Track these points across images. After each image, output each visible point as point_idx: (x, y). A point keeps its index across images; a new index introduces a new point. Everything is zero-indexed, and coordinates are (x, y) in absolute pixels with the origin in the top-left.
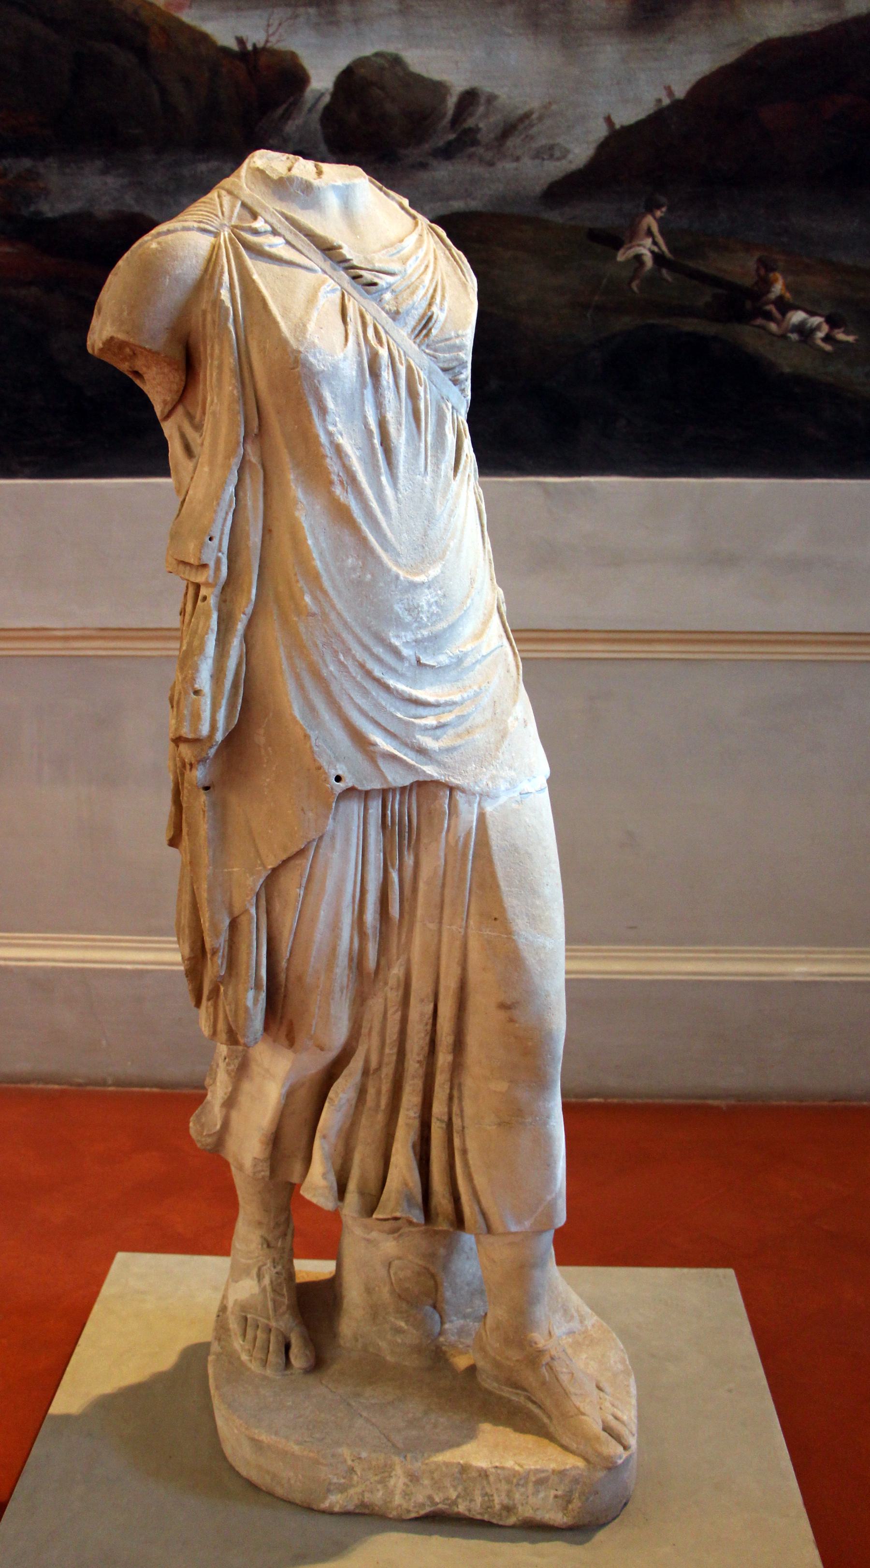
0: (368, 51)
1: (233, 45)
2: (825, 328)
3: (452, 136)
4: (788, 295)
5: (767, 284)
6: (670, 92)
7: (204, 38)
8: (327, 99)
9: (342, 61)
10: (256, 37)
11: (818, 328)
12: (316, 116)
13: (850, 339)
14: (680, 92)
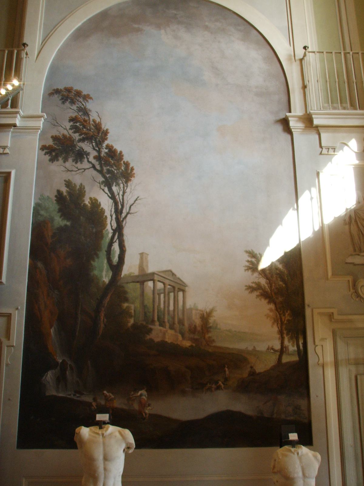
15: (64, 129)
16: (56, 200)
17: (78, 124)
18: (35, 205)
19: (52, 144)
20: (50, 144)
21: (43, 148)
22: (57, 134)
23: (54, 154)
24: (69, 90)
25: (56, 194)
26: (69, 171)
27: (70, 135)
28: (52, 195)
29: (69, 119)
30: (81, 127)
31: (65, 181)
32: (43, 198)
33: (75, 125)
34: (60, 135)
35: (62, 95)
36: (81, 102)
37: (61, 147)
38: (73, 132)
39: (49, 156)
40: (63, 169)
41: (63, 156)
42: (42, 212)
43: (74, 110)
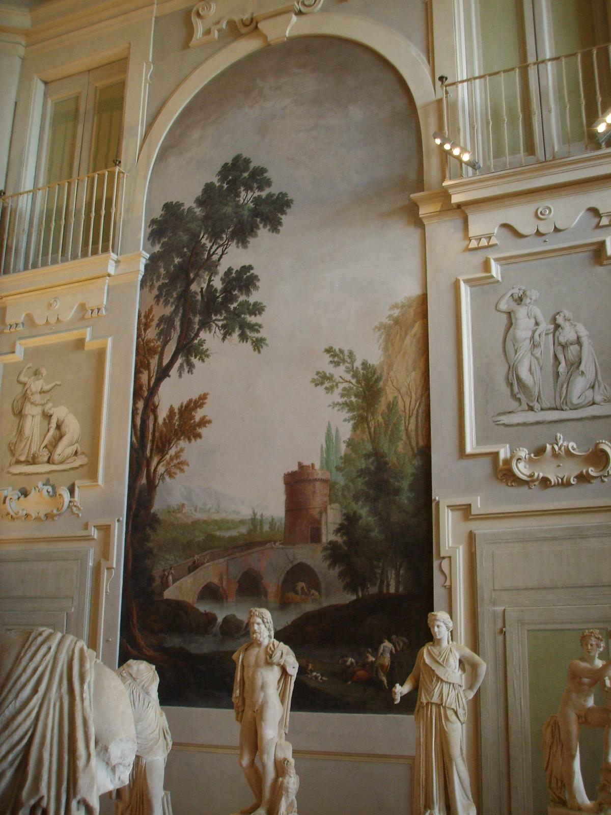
0: (229, 613)
1: (204, 612)
2: (320, 677)
3: (244, 632)
4: (313, 669)
5: (308, 666)
6: (287, 623)
7: (198, 610)
8: (221, 624)
9: (224, 616)
10: (208, 610)
11: (319, 676)
12: (218, 628)
13: (326, 679)
14: (290, 623)
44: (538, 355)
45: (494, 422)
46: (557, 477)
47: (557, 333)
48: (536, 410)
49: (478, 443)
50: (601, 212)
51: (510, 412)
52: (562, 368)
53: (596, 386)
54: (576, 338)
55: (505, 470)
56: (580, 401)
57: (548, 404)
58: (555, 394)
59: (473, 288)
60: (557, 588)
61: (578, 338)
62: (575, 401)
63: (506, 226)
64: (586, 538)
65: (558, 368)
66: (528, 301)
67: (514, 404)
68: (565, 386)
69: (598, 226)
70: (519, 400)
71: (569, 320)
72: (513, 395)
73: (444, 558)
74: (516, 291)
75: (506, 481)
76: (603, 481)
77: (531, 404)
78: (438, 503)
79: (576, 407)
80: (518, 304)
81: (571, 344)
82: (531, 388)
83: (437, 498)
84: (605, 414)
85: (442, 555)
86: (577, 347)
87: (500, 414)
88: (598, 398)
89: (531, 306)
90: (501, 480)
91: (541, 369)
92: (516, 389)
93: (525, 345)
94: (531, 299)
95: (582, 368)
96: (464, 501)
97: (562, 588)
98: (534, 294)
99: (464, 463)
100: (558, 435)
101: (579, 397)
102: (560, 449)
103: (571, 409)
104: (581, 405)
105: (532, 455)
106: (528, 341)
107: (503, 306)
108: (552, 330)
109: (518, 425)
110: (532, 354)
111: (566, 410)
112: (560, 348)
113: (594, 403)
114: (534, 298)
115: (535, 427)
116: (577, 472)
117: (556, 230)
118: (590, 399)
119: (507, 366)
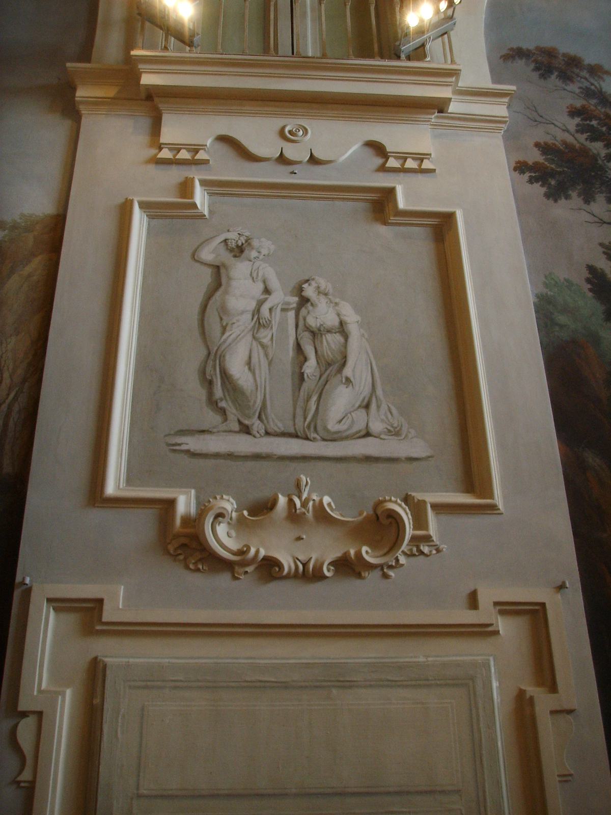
15: (564, 130)
16: (590, 290)
17: (594, 123)
18: (536, 300)
19: (543, 161)
20: (536, 160)
21: (520, 167)
22: (549, 140)
23: (553, 182)
24: (550, 53)
25: (586, 274)
26: (605, 222)
27: (582, 144)
28: (579, 277)
29: (568, 110)
30: (604, 129)
31: (601, 245)
32: (553, 282)
33: (588, 125)
34: (557, 143)
35: (536, 61)
36: (586, 79)
37: (566, 167)
38: (586, 139)
39: (542, 186)
40: (589, 218)
41: (579, 188)
42: (562, 319)
43: (574, 93)
44: (266, 341)
45: (169, 445)
46: (296, 559)
47: (303, 311)
48: (255, 432)
49: (129, 481)
50: (388, 150)
51: (203, 432)
52: (311, 367)
53: (373, 406)
54: (337, 323)
55: (186, 536)
56: (342, 427)
57: (280, 425)
58: (295, 409)
59: (155, 222)
60: (286, 795)
61: (342, 323)
62: (332, 426)
63: (224, 139)
64: (350, 687)
65: (301, 368)
66: (254, 254)
67: (211, 418)
68: (314, 398)
69: (383, 169)
70: (223, 412)
71: (326, 294)
72: (212, 403)
73: (24, 714)
74: (232, 236)
75: (185, 559)
76: (385, 576)
77: (246, 422)
78: (28, 592)
79: (335, 436)
80: (235, 256)
81: (329, 331)
82: (248, 393)
83: (28, 581)
84: (388, 455)
85: (22, 707)
86: (339, 338)
87: (182, 432)
88: (377, 426)
89: (257, 263)
90: (175, 557)
91: (270, 364)
92: (218, 392)
93: (245, 322)
94: (259, 252)
95: (348, 371)
96: (89, 591)
97: (296, 795)
98: (265, 245)
99: (97, 516)
100: (304, 478)
101: (340, 421)
102: (304, 504)
103: (324, 440)
104: (345, 434)
105: (245, 513)
106: (249, 316)
107: (207, 255)
108: (295, 305)
109: (217, 456)
110: (254, 337)
111: (314, 440)
112: (307, 335)
113: (368, 434)
114: (264, 251)
115: (250, 464)
116: (335, 554)
117: (313, 160)
118: (360, 426)
119: (205, 352)
